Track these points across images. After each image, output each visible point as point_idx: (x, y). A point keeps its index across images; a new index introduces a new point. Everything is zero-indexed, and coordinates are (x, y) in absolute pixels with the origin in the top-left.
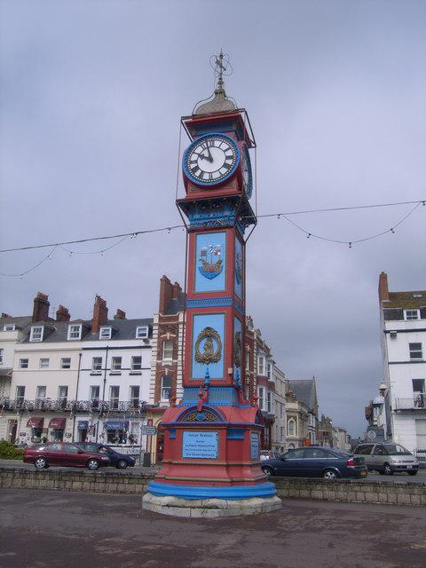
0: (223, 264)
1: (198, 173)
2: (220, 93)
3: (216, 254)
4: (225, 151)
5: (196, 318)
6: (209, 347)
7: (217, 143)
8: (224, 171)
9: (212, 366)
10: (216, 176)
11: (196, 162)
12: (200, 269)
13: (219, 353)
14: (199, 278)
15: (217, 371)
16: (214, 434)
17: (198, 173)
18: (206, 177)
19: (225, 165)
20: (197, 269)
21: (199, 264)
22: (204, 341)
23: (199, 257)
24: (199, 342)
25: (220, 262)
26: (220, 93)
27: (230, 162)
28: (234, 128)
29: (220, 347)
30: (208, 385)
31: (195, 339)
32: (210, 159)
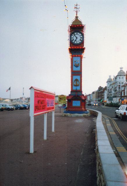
0: (80, 64)
2: (77, 17)
5: (73, 76)
6: (77, 83)
7: (78, 34)
8: (80, 41)
11: (73, 38)
12: (74, 65)
15: (78, 88)
19: (80, 40)
21: (74, 64)
24: (74, 83)
25: (79, 64)
26: (77, 17)
27: (81, 39)
31: (73, 81)
32: (77, 38)
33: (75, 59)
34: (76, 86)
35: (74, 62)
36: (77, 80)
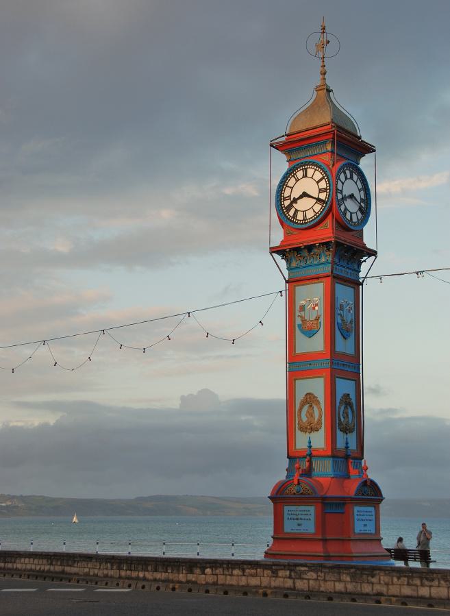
1: (292, 213)
3: (314, 308)
4: (318, 182)
6: (311, 414)
9: (314, 435)
10: (310, 215)
13: (320, 420)
14: (298, 334)
16: (312, 509)
17: (292, 213)
18: (300, 216)
20: (297, 327)
21: (298, 321)
22: (306, 407)
23: (297, 313)
24: (300, 409)
25: (317, 319)
28: (329, 148)
29: (320, 415)
30: (311, 455)
33: (302, 291)
34: (311, 428)
35: (297, 308)
36: (310, 399)
